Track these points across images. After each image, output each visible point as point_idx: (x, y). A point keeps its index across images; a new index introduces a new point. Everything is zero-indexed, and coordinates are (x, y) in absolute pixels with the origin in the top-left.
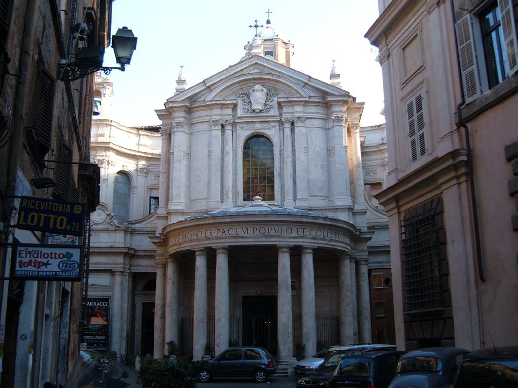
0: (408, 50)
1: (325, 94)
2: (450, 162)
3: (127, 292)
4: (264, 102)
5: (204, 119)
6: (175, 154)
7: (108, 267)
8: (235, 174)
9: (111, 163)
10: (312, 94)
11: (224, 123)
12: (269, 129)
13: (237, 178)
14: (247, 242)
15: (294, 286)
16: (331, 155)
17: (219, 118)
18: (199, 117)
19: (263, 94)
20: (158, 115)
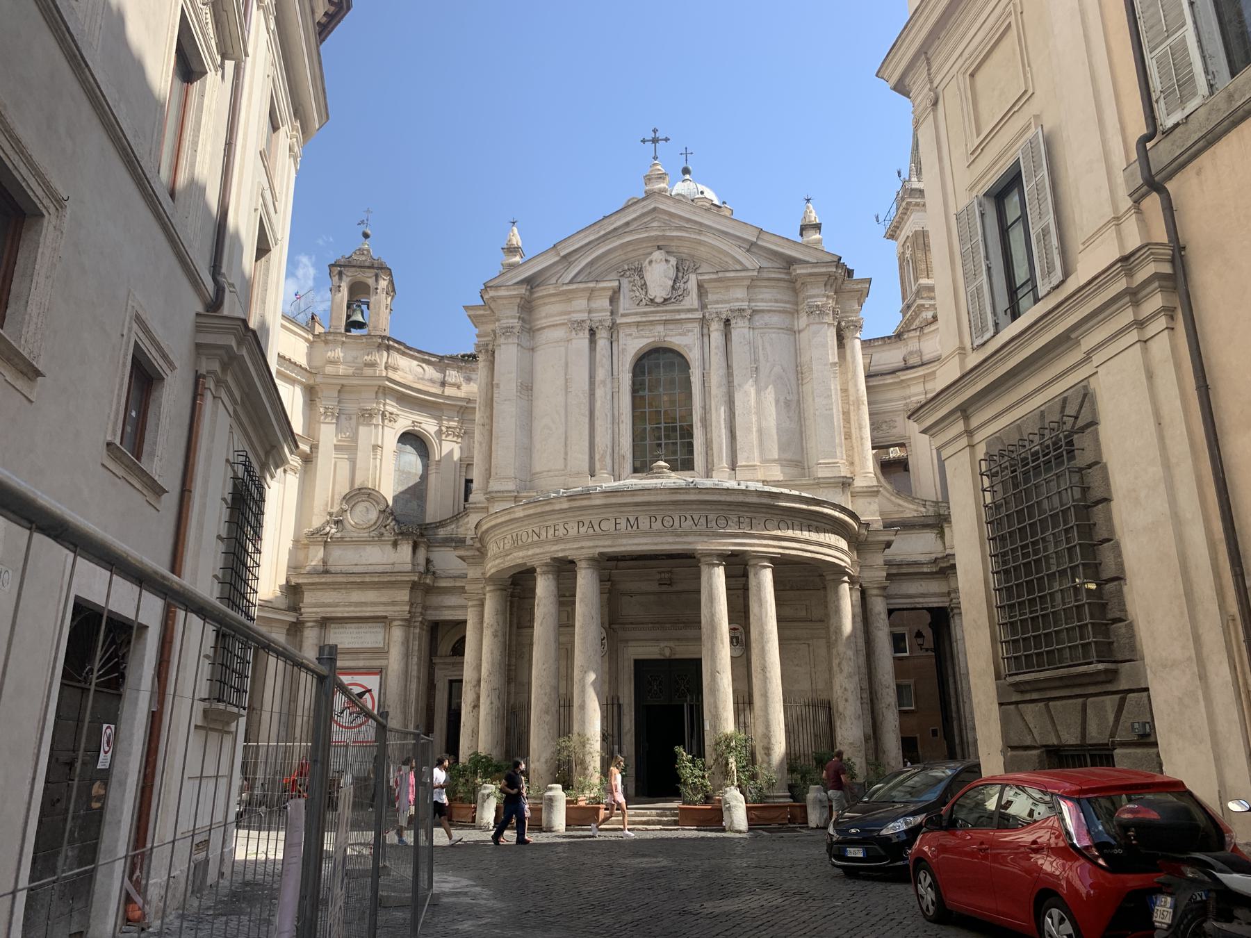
0: (979, 77)
1: (790, 262)
2: (1121, 285)
3: (415, 659)
4: (671, 283)
5: (558, 320)
6: (501, 386)
7: (380, 611)
8: (615, 421)
9: (388, 415)
10: (765, 264)
12: (680, 335)
14: (636, 544)
15: (737, 638)
16: (805, 381)
17: (585, 316)
18: (546, 317)
19: (669, 268)
20: (469, 316)
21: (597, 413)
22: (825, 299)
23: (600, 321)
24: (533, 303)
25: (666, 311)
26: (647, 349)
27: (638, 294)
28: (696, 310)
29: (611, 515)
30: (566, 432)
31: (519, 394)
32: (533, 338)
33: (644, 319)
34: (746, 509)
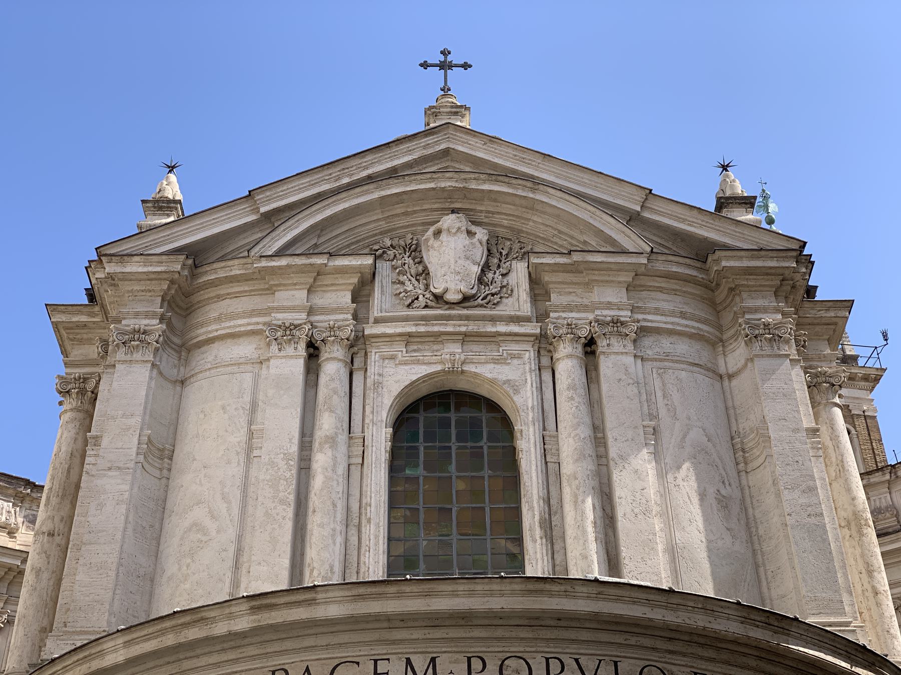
4: (476, 270)
5: (241, 324)
6: (105, 442)
11: (317, 337)
13: (364, 537)
18: (219, 319)
20: (56, 325)
21: (315, 500)
22: (779, 316)
23: (331, 328)
24: (196, 298)
25: (468, 318)
26: (424, 390)
27: (410, 287)
28: (528, 320)
29: (365, 651)
30: (240, 538)
31: (141, 458)
32: (187, 362)
33: (422, 329)
34: (711, 653)
